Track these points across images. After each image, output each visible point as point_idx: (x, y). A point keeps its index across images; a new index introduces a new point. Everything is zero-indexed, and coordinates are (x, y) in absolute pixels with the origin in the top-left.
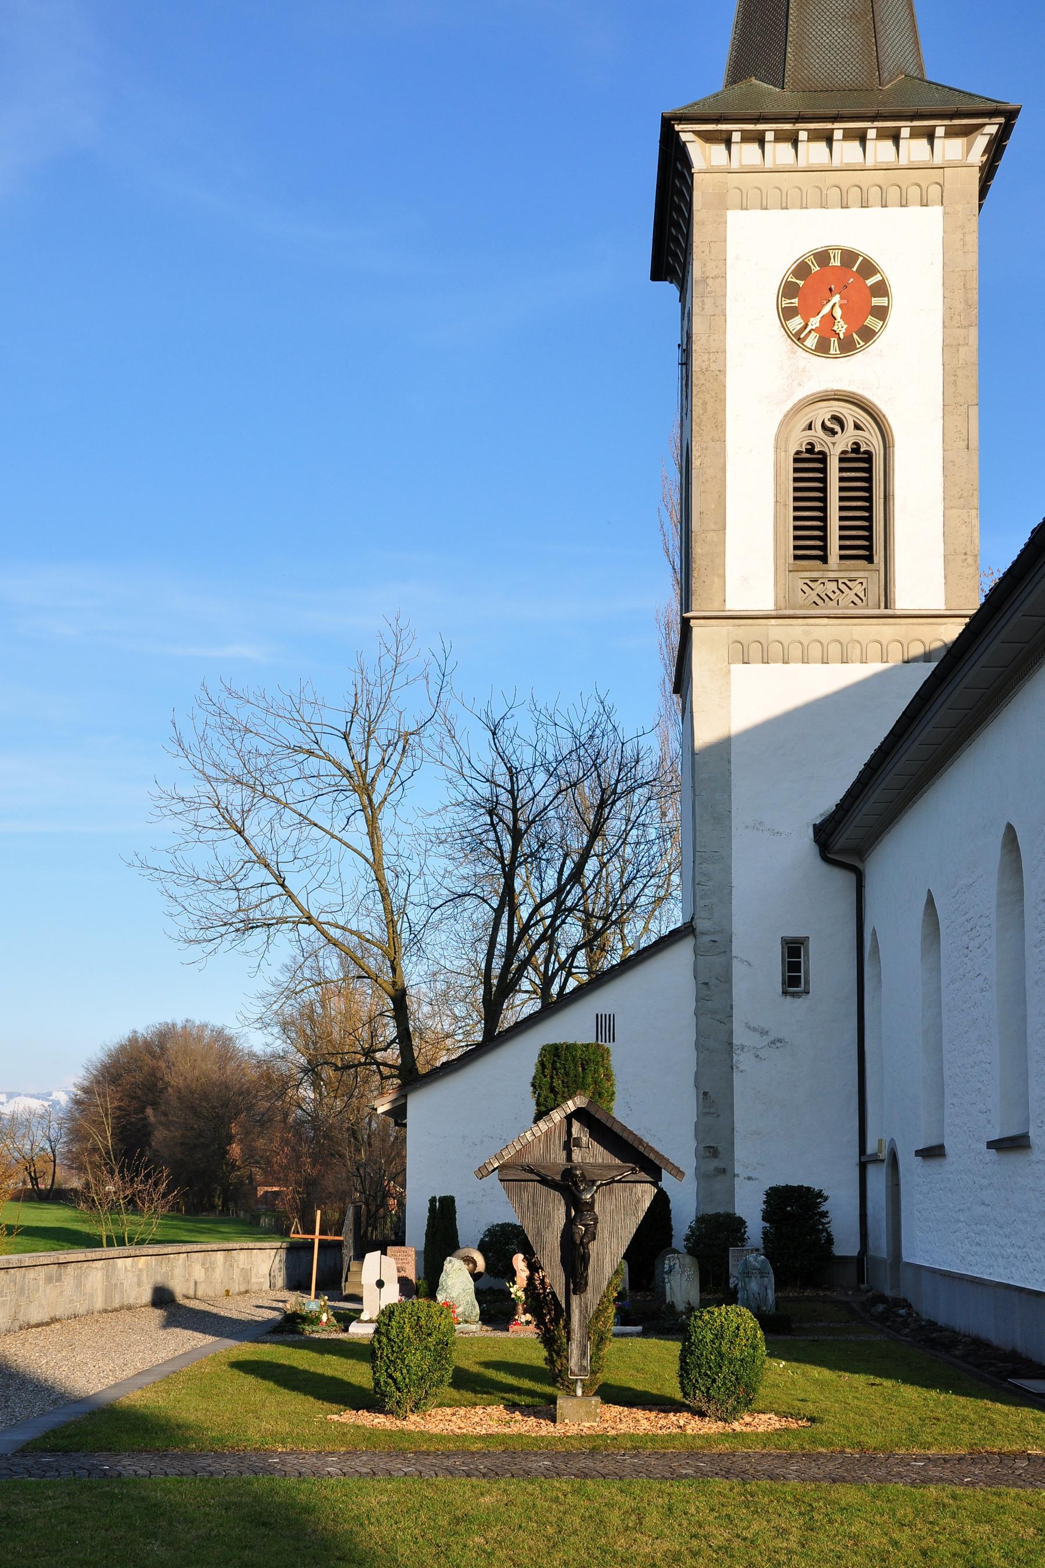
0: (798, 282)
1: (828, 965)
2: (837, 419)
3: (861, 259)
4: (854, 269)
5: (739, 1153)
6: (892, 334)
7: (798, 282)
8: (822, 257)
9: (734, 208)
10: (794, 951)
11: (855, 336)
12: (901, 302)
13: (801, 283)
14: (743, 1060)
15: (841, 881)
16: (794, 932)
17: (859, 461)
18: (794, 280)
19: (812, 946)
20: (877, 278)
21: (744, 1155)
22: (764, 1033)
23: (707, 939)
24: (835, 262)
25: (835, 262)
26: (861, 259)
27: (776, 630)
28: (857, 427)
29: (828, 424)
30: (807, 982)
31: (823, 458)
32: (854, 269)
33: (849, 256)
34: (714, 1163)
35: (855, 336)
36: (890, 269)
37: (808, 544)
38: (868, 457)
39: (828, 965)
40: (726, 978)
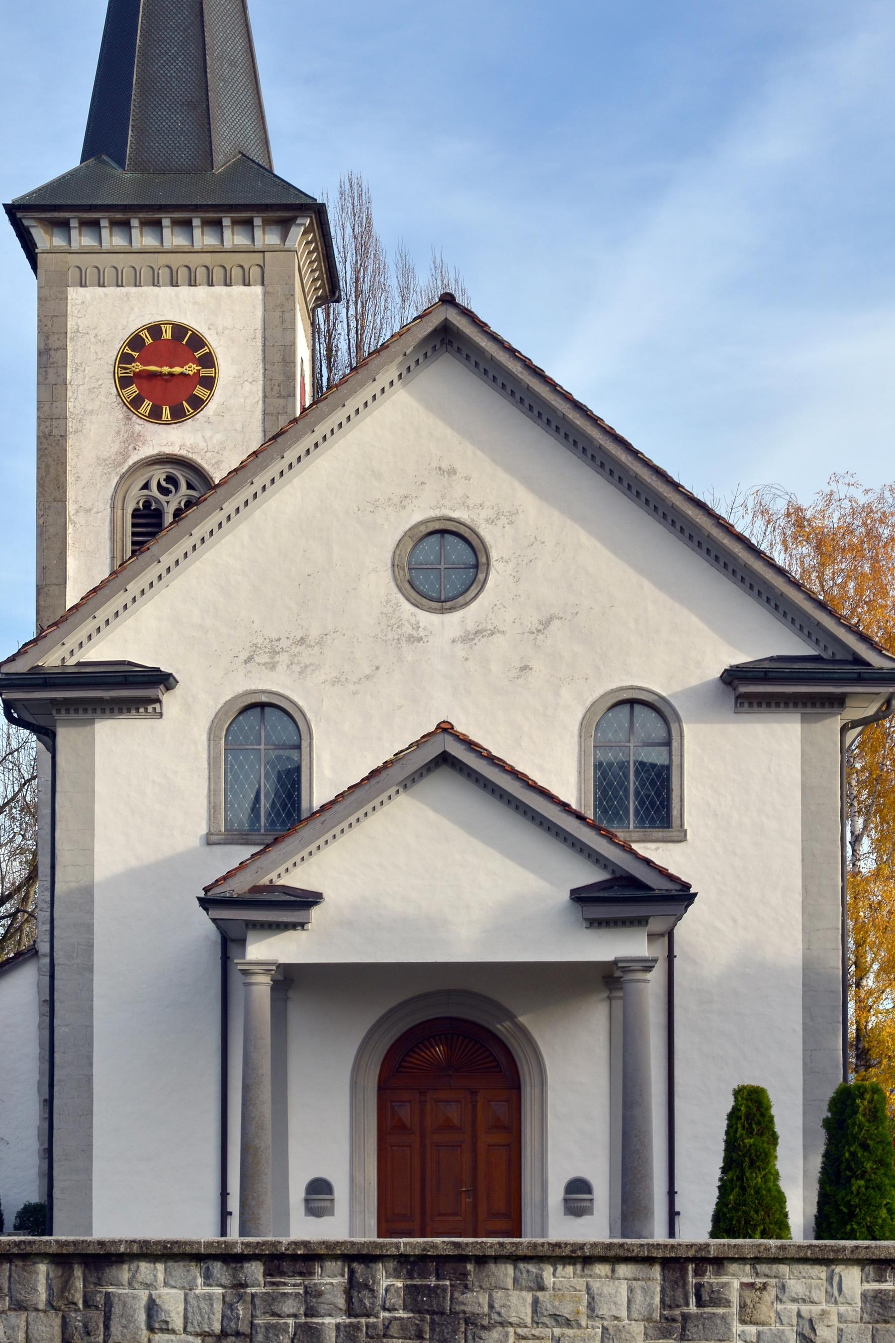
0: (133, 353)
3: (190, 333)
4: (184, 342)
7: (133, 353)
8: (155, 330)
9: (73, 285)
11: (185, 404)
12: (226, 370)
13: (136, 354)
18: (130, 352)
20: (206, 350)
24: (167, 334)
25: (167, 334)
26: (190, 333)
28: (190, 486)
29: (163, 483)
32: (184, 342)
33: (179, 330)
35: (185, 404)
36: (215, 343)
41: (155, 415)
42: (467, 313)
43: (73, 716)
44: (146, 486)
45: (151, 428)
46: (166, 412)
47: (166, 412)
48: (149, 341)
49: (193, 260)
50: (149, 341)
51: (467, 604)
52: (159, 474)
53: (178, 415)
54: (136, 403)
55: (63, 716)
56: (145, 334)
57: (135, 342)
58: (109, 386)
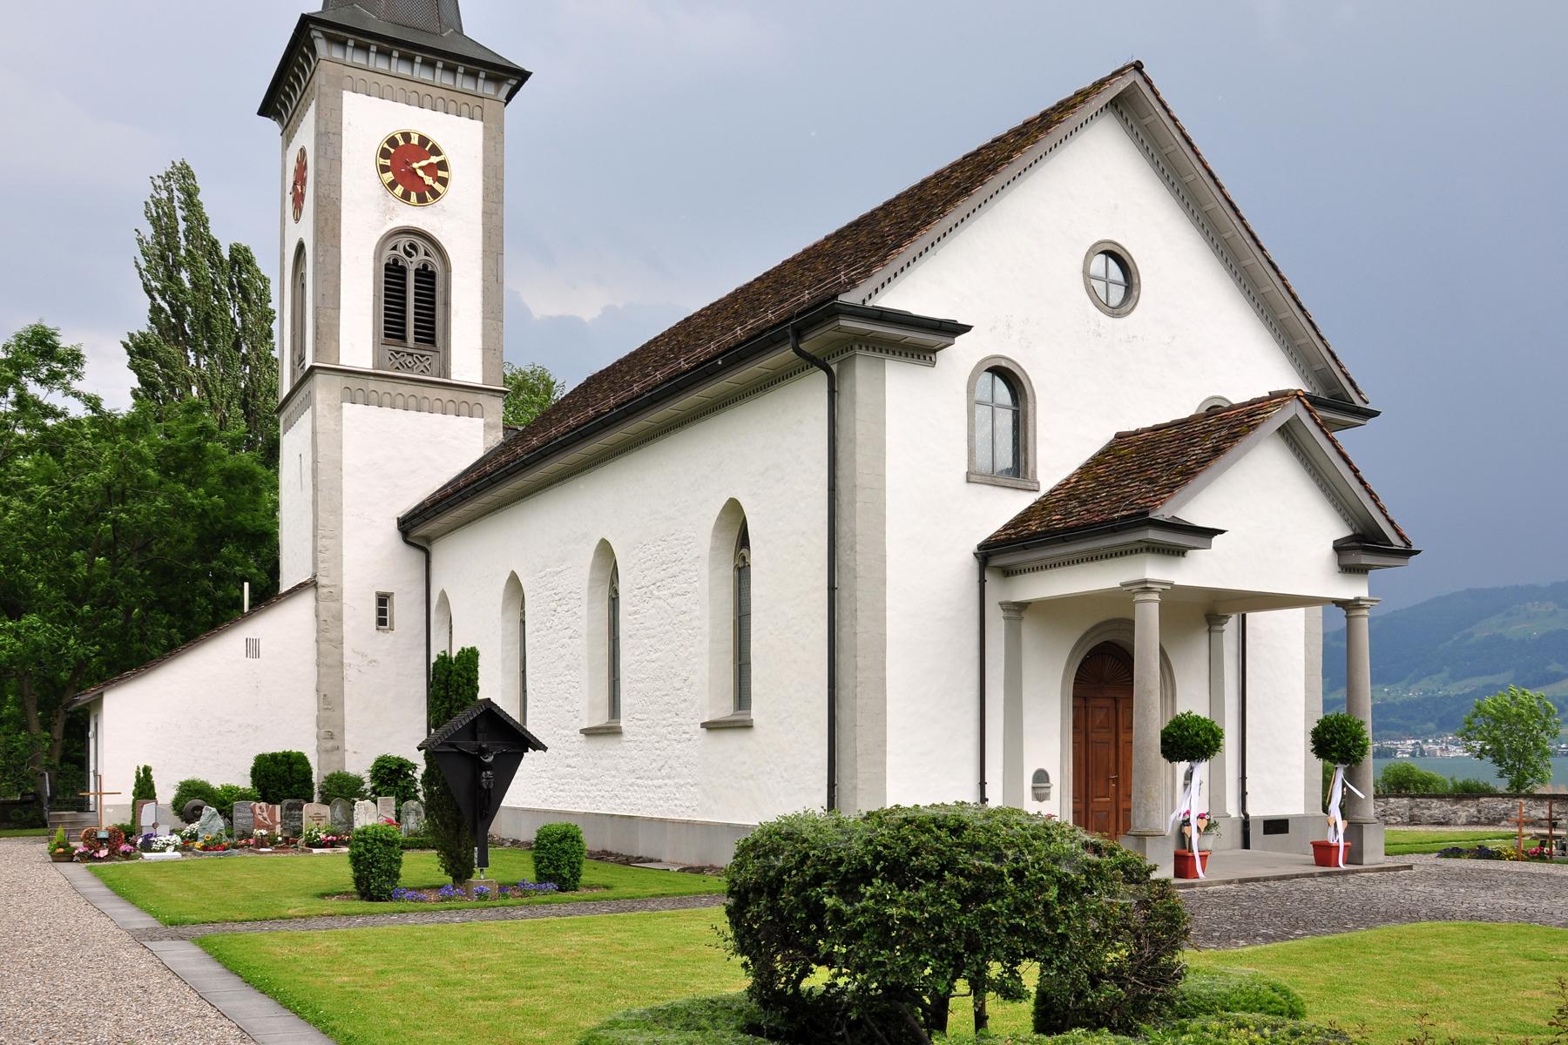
1: (406, 611)
2: (412, 246)
5: (348, 737)
6: (450, 195)
8: (406, 136)
10: (383, 600)
12: (455, 174)
14: (350, 673)
15: (416, 556)
16: (383, 590)
17: (426, 277)
19: (396, 599)
21: (350, 739)
22: (363, 655)
23: (325, 590)
24: (415, 141)
25: (415, 141)
27: (372, 385)
30: (392, 623)
31: (403, 270)
33: (424, 140)
34: (330, 744)
36: (448, 154)
37: (392, 327)
38: (432, 275)
39: (406, 611)
40: (339, 618)
41: (406, 196)
42: (1148, 81)
43: (870, 353)
44: (395, 248)
45: (402, 206)
46: (413, 196)
47: (413, 196)
48: (401, 143)
49: (436, 92)
50: (401, 143)
51: (1128, 313)
52: (404, 241)
53: (422, 200)
54: (392, 185)
55: (863, 352)
56: (398, 137)
57: (392, 141)
58: (373, 170)
